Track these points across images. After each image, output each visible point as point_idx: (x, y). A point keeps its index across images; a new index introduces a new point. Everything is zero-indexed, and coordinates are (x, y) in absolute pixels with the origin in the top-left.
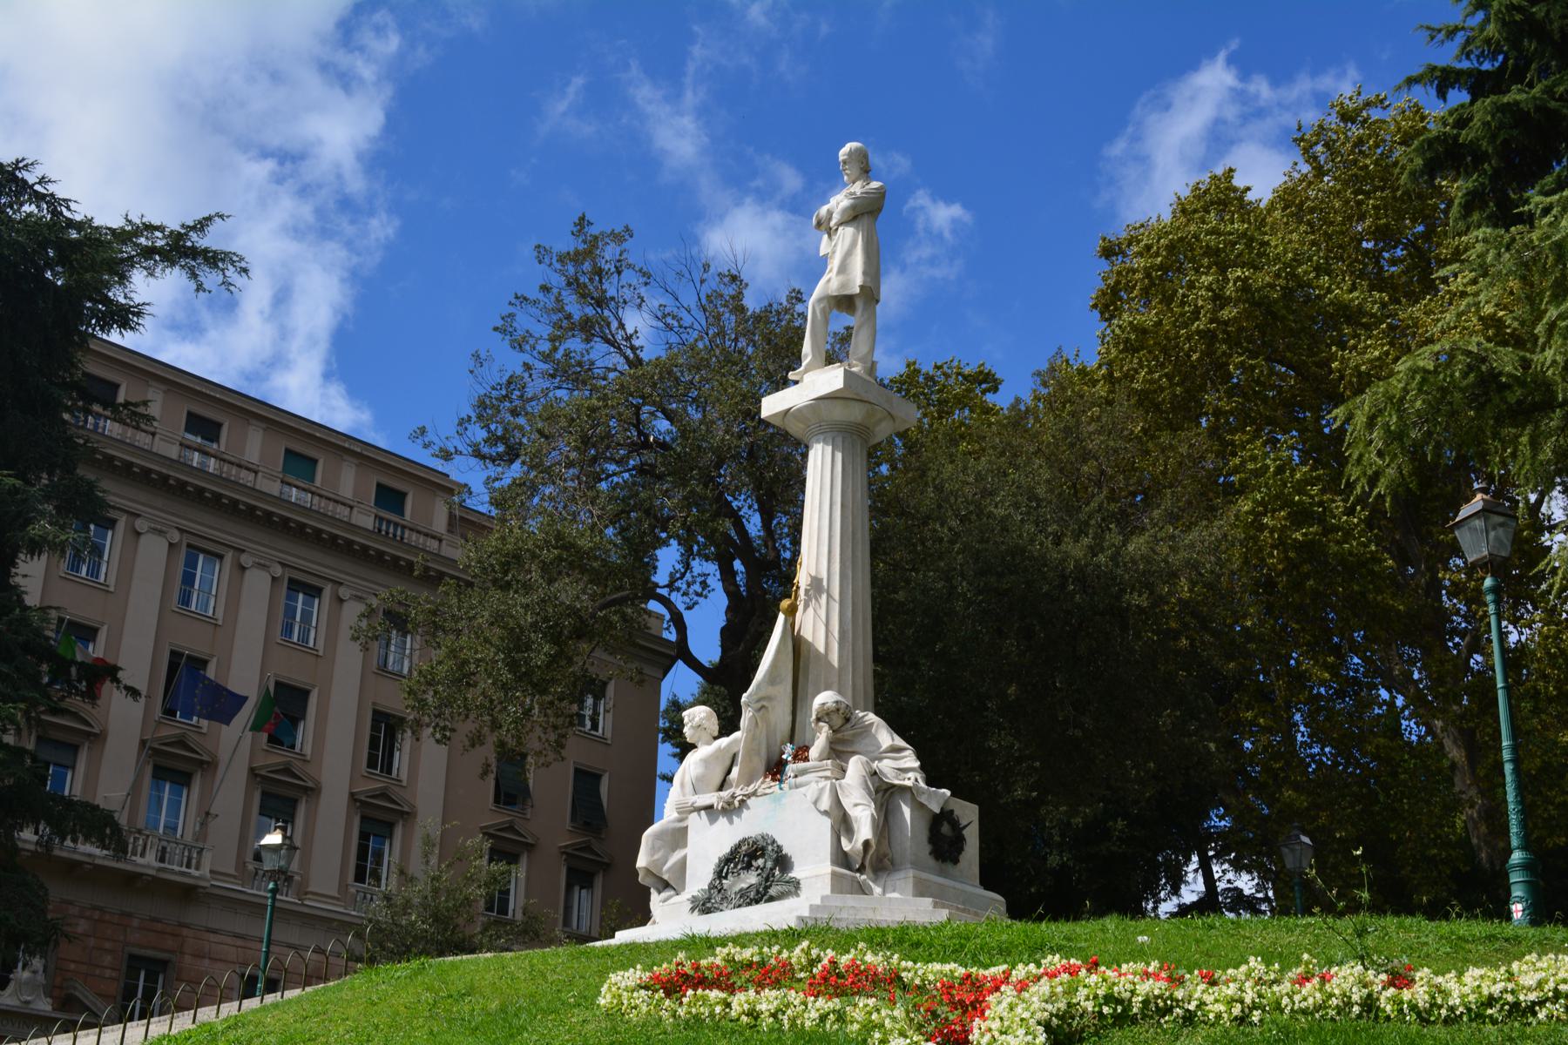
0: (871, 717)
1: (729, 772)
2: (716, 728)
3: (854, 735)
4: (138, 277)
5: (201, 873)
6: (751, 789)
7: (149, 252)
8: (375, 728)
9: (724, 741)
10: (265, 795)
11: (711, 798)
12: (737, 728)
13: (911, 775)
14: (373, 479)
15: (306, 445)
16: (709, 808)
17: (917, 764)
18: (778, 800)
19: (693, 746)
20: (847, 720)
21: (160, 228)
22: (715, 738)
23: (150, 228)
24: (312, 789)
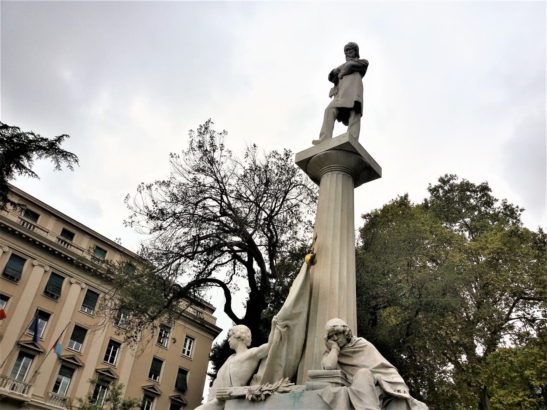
0: (363, 341)
1: (256, 371)
2: (250, 340)
3: (354, 352)
4: (34, 155)
5: (27, 397)
6: (274, 387)
7: (41, 148)
8: (110, 346)
9: (255, 350)
10: (63, 367)
11: (243, 390)
12: (267, 342)
13: (399, 388)
14: (126, 260)
15: (103, 244)
16: (242, 398)
17: (402, 380)
18: (297, 397)
19: (233, 352)
20: (349, 341)
21: (46, 140)
22: (249, 348)
23: (43, 139)
24: (81, 366)
